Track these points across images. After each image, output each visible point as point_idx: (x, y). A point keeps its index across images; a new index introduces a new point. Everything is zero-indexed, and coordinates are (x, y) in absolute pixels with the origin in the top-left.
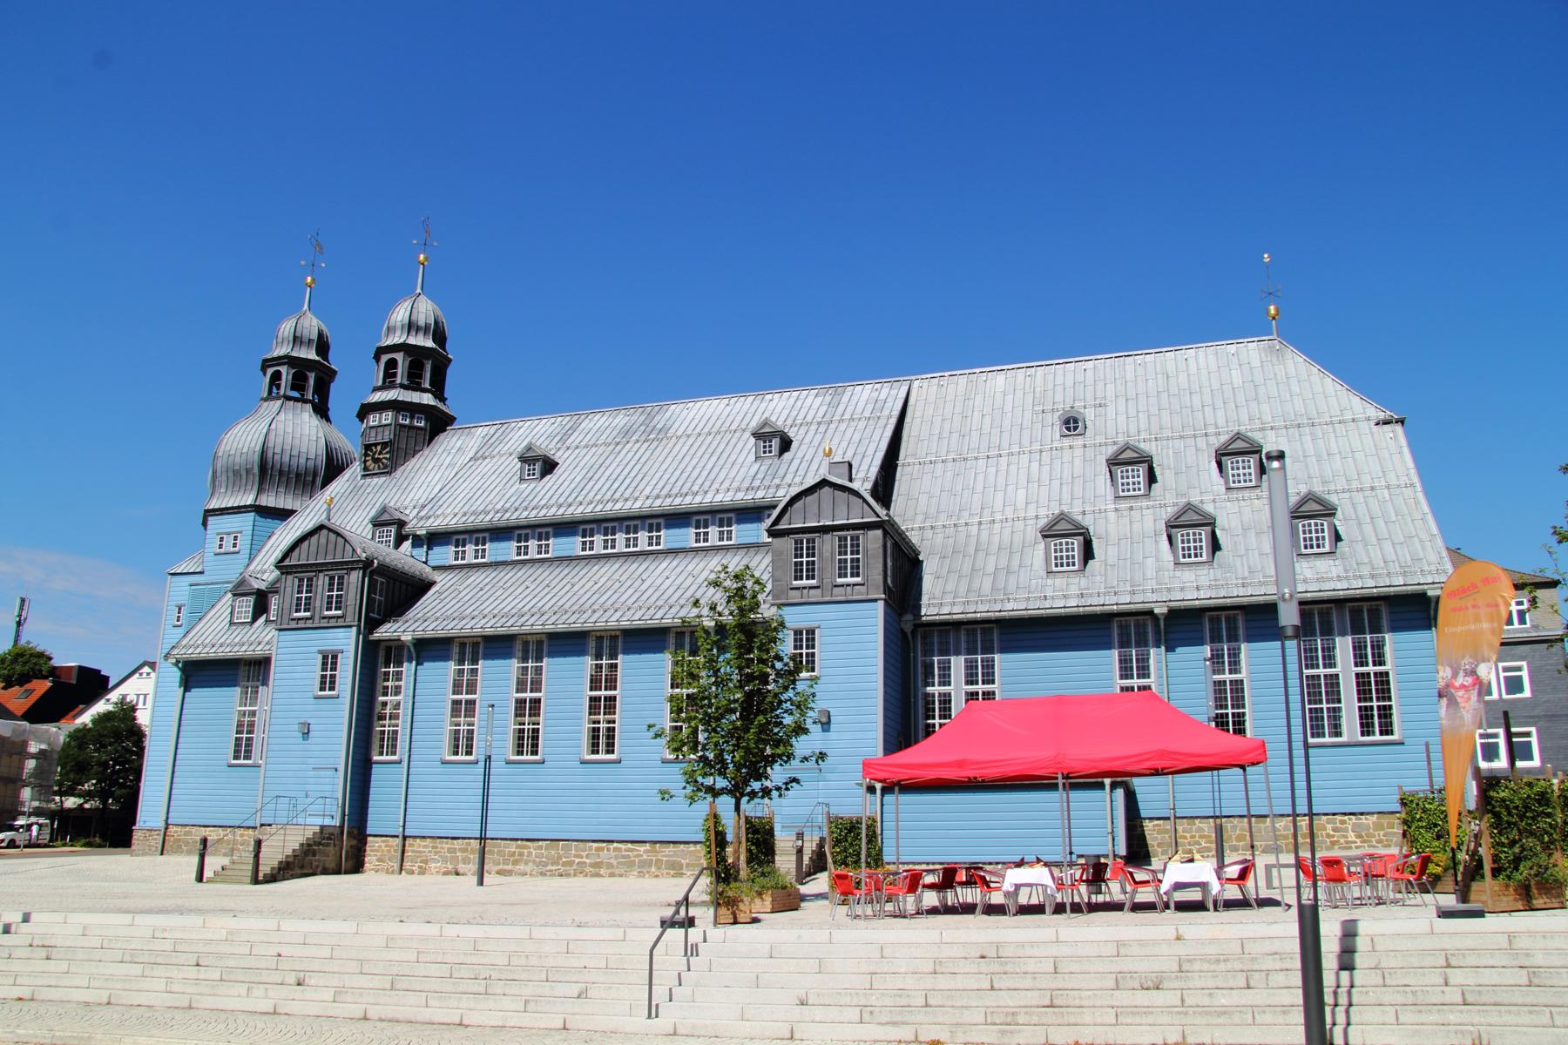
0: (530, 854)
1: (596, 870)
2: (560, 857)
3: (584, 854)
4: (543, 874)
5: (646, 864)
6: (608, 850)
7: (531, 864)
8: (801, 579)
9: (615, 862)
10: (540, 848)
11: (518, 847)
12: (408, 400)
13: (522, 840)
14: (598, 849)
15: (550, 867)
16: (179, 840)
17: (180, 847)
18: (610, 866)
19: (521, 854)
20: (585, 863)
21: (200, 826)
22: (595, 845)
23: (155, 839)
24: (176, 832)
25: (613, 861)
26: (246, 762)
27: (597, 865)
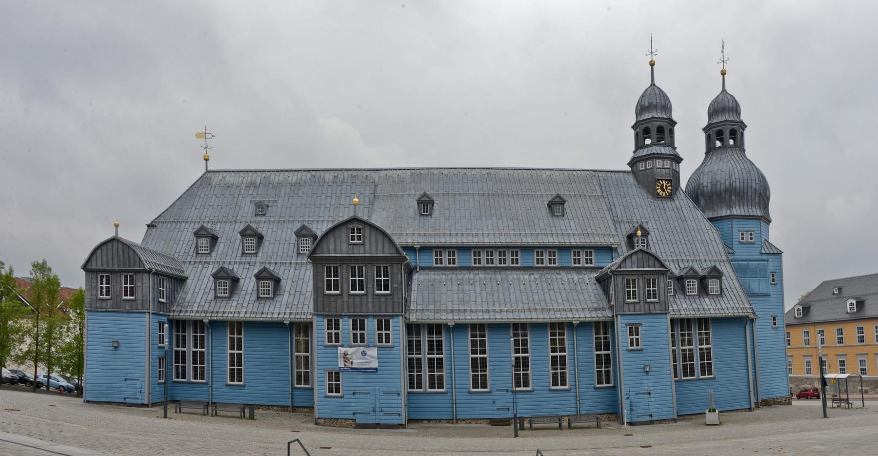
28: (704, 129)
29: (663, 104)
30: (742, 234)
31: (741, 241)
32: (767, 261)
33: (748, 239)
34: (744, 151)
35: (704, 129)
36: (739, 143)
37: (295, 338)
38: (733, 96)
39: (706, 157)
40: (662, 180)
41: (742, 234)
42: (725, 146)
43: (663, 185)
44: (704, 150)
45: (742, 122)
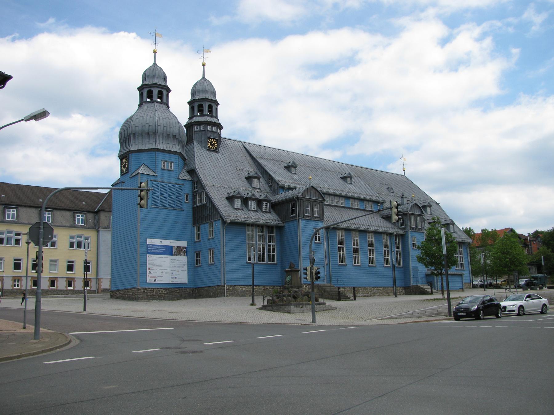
0: (360, 291)
1: (374, 295)
2: (366, 292)
3: (371, 290)
4: (364, 296)
5: (382, 293)
6: (375, 289)
7: (361, 294)
8: (401, 226)
9: (377, 292)
10: (361, 289)
11: (357, 289)
12: (203, 120)
13: (358, 287)
14: (373, 289)
15: (365, 295)
16: (231, 291)
17: (232, 294)
18: (376, 293)
19: (358, 291)
20: (371, 293)
21: (238, 286)
22: (372, 288)
23: (150, 292)
24: (229, 288)
25: (376, 292)
26: (273, 263)
27: (374, 293)
28: (138, 89)
29: (212, 91)
30: (164, 163)
31: (163, 168)
32: (183, 185)
33: (168, 167)
34: (169, 107)
35: (138, 89)
36: (165, 101)
37: (258, 233)
38: (161, 68)
39: (139, 107)
40: (211, 139)
41: (164, 163)
42: (152, 102)
43: (213, 142)
44: (137, 103)
45: (217, 101)
